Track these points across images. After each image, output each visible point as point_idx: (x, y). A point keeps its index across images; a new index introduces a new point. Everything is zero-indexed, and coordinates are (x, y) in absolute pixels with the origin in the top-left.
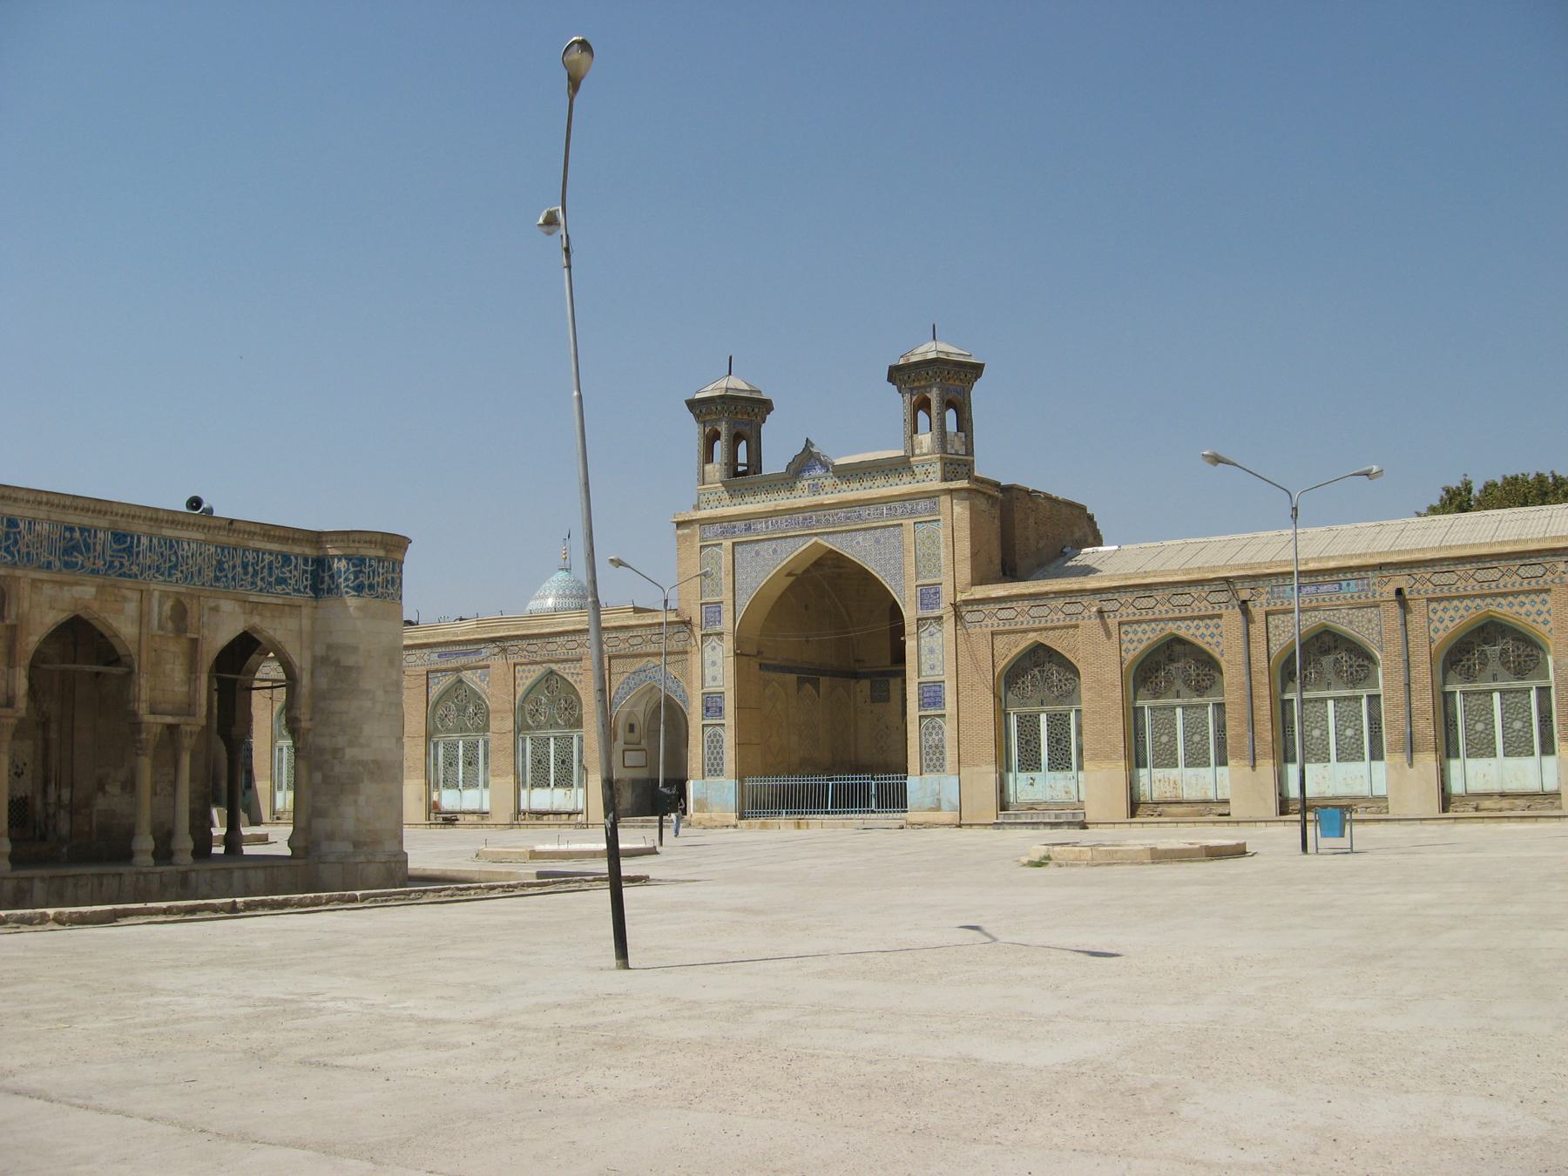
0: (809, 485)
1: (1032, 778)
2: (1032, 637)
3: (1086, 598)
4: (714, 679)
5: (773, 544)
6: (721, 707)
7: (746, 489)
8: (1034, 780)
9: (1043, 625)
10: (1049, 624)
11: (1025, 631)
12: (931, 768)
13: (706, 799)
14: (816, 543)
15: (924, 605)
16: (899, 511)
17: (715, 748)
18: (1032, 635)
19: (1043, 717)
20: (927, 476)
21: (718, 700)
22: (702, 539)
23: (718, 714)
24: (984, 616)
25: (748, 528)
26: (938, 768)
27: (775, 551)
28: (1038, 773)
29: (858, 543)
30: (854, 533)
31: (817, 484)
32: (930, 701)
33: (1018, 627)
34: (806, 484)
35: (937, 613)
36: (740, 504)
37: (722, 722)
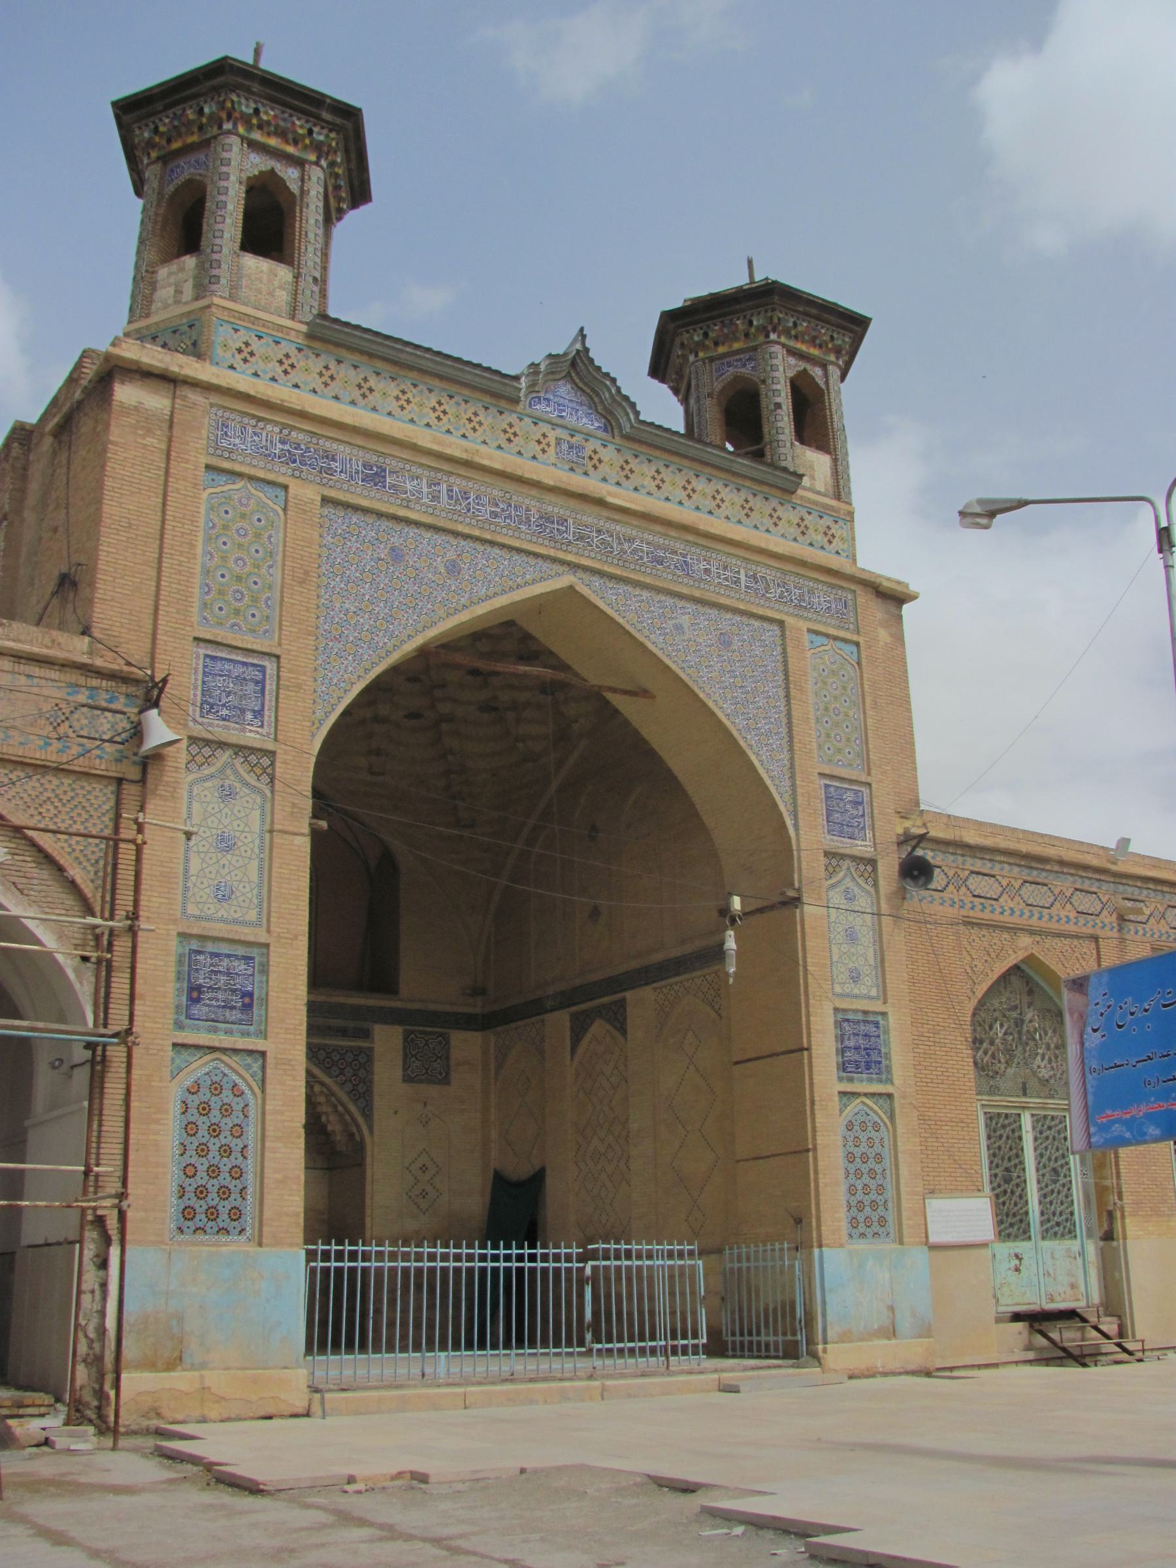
0: (559, 441)
1: (1017, 1256)
2: (1023, 946)
3: (1105, 886)
4: (224, 895)
5: (452, 549)
6: (250, 995)
7: (378, 374)
8: (1021, 1260)
9: (1044, 924)
10: (1053, 926)
11: (1014, 930)
12: (862, 1228)
13: (181, 1319)
14: (571, 588)
15: (836, 827)
16: (774, 593)
17: (215, 1130)
18: (1025, 941)
19: (1026, 1121)
20: (830, 542)
21: (240, 967)
22: (215, 448)
23: (236, 1015)
24: (946, 880)
25: (376, 477)
26: (876, 1227)
27: (453, 569)
28: (1025, 1244)
29: (679, 628)
30: (670, 601)
31: (580, 448)
32: (856, 1057)
33: (1006, 918)
34: (552, 436)
35: (862, 847)
36: (353, 403)
37: (259, 1044)
